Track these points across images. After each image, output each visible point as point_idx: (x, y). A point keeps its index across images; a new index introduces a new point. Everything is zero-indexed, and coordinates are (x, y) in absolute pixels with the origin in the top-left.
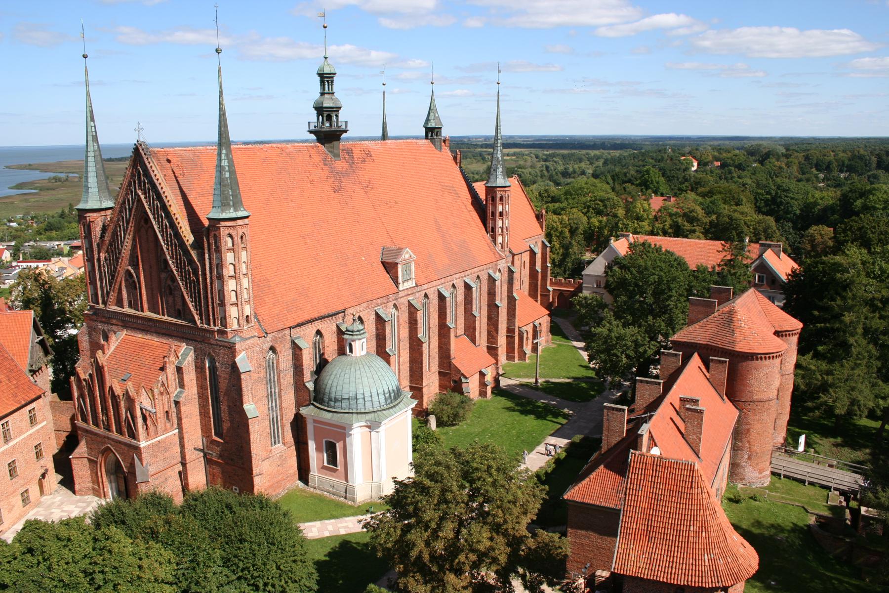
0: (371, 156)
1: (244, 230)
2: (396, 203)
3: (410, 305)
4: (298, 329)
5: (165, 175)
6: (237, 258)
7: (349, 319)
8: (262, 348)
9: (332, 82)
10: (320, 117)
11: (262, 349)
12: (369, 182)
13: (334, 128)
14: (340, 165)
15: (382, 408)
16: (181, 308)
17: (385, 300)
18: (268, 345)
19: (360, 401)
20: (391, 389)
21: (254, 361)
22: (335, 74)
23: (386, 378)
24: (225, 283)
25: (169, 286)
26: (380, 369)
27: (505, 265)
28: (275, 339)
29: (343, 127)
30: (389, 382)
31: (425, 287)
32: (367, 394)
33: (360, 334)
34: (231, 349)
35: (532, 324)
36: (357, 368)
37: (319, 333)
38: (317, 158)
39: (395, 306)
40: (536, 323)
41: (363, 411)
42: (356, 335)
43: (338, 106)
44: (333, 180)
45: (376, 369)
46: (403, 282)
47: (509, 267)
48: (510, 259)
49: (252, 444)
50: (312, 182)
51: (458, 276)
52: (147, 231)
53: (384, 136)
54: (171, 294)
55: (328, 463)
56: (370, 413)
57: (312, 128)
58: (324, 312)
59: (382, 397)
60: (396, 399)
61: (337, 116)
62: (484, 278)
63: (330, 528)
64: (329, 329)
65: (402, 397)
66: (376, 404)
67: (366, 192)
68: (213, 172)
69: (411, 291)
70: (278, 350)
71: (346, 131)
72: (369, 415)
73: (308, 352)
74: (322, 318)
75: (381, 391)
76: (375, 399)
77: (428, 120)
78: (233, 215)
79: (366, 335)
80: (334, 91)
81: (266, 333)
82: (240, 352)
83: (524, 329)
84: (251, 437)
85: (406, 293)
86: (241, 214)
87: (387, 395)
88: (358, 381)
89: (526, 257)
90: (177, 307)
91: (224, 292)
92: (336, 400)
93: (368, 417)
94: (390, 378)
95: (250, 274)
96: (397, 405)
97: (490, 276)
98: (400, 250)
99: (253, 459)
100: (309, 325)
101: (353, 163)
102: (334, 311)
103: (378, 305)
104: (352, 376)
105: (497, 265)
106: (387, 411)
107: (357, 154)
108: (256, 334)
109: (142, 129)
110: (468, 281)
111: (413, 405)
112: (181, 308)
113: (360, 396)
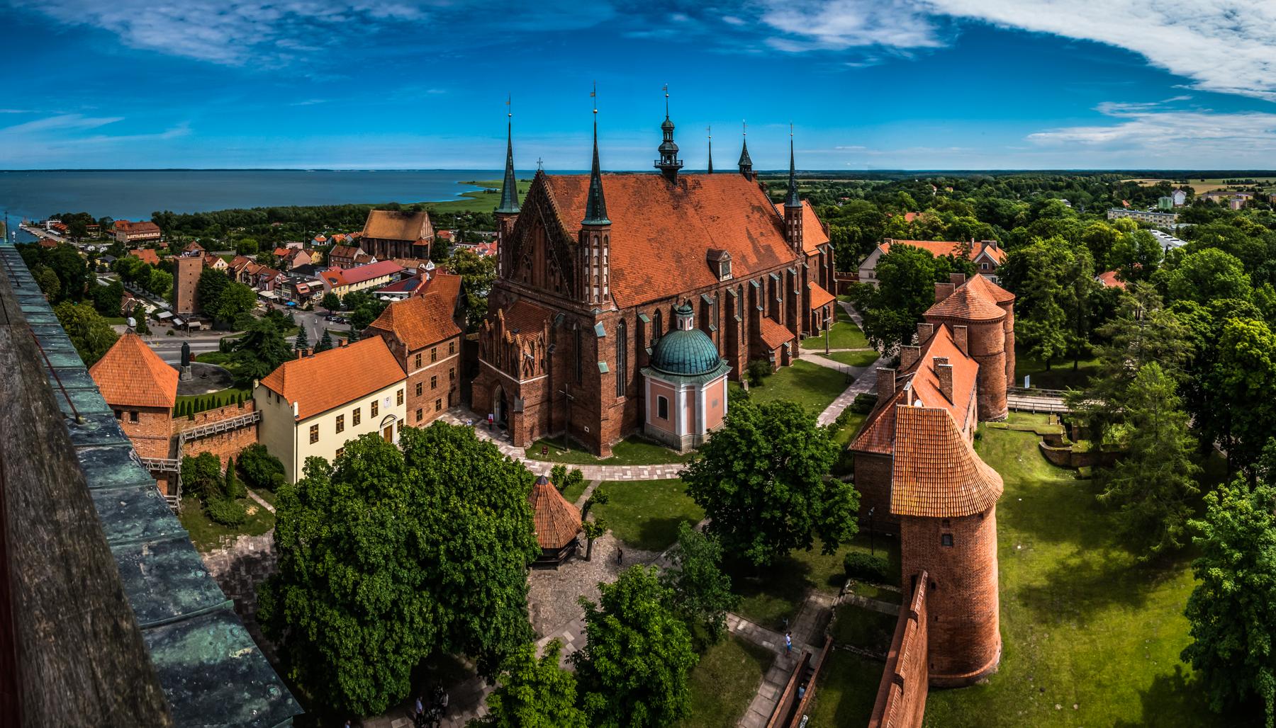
1: (607, 233)
3: (727, 293)
6: (601, 253)
7: (681, 301)
18: (619, 318)
19: (688, 366)
28: (625, 314)
32: (693, 360)
34: (592, 319)
37: (658, 311)
39: (717, 294)
59: (704, 364)
60: (715, 365)
62: (784, 273)
64: (665, 309)
66: (700, 369)
68: (587, 191)
69: (731, 282)
74: (661, 300)
75: (703, 358)
76: (699, 365)
78: (599, 223)
86: (605, 222)
92: (669, 364)
93: (693, 379)
110: (772, 275)
113: (687, 362)
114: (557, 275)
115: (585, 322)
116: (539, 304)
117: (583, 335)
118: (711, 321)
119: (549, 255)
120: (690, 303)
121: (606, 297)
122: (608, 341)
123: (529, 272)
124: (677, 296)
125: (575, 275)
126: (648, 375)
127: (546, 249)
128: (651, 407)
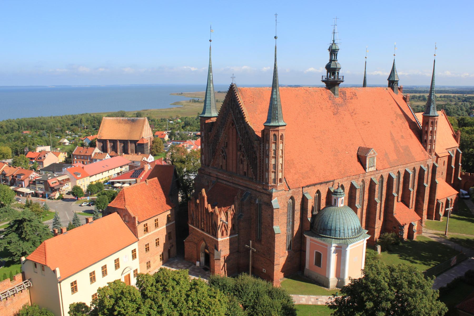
0: (356, 95)
2: (369, 122)
4: (306, 188)
5: (244, 101)
8: (286, 197)
9: (337, 54)
10: (329, 73)
11: (286, 197)
12: (354, 110)
13: (336, 79)
14: (338, 99)
15: (350, 237)
16: (246, 171)
17: (357, 177)
18: (290, 196)
19: (338, 232)
20: (356, 227)
21: (282, 203)
22: (338, 50)
23: (354, 221)
24: (270, 160)
25: (241, 159)
26: (351, 215)
27: (432, 162)
28: (294, 192)
29: (341, 79)
30: (355, 223)
31: (382, 171)
32: (342, 228)
33: (341, 195)
34: (270, 196)
35: (446, 199)
36: (338, 213)
37: (318, 192)
38: (325, 96)
40: (449, 199)
41: (338, 238)
42: (339, 195)
43: (340, 67)
44: (333, 108)
45: (348, 215)
46: (369, 167)
47: (434, 164)
48: (435, 159)
49: (275, 248)
50: (322, 108)
51: (402, 166)
52: (233, 130)
53: (364, 85)
54: (242, 163)
55: (315, 264)
56: (343, 239)
57: (324, 79)
58: (322, 180)
59: (350, 231)
60: (358, 233)
61: (338, 73)
63: (313, 300)
65: (362, 232)
66: (346, 235)
67: (352, 116)
70: (295, 198)
71: (343, 81)
72: (342, 240)
73: (311, 202)
74: (321, 183)
76: (346, 231)
77: (390, 76)
78: (277, 124)
79: (345, 195)
80: (337, 59)
81: (290, 189)
82: (275, 197)
83: (440, 201)
84: (275, 244)
85: (370, 173)
87: (353, 231)
88: (338, 221)
89: (446, 159)
90: (244, 170)
91: (269, 164)
93: (341, 241)
94: (356, 221)
95: (283, 156)
96: (358, 237)
97: (421, 168)
98: (368, 150)
99: (275, 256)
100: (313, 187)
101: (346, 99)
102: (328, 181)
103: (353, 179)
104: (334, 217)
105: (426, 162)
106: (352, 239)
107: (348, 94)
108: (284, 189)
109: (235, 77)
110: (408, 170)
111: (368, 238)
112: (246, 171)
113: (338, 229)
114: (245, 163)
115: (265, 198)
116: (231, 184)
117: (263, 207)
118: (357, 201)
119: (239, 148)
120: (342, 187)
121: (281, 180)
122: (281, 211)
123: (224, 161)
124: (333, 181)
125: (258, 164)
126: (309, 239)
127: (237, 144)
128: (309, 258)
